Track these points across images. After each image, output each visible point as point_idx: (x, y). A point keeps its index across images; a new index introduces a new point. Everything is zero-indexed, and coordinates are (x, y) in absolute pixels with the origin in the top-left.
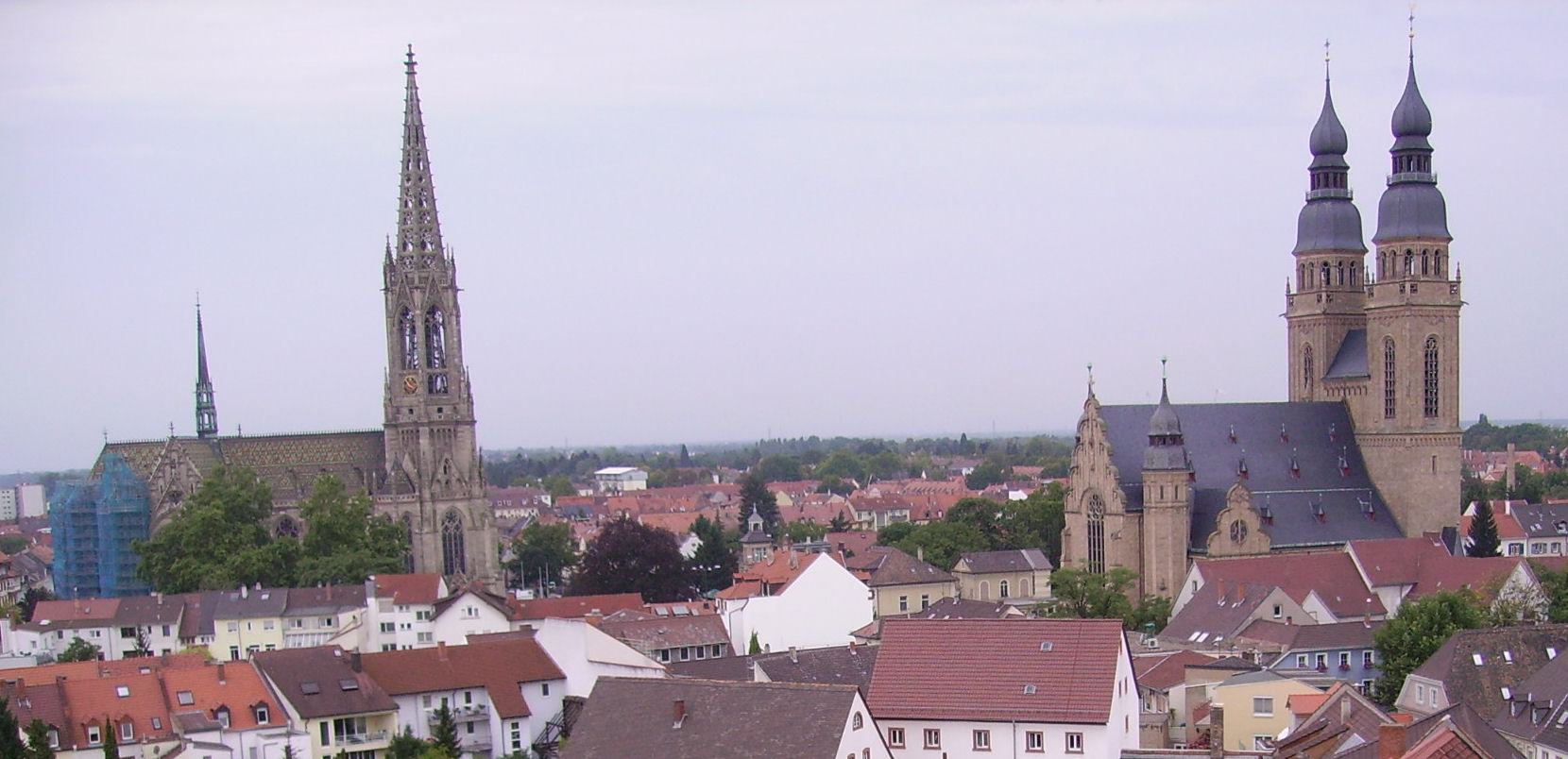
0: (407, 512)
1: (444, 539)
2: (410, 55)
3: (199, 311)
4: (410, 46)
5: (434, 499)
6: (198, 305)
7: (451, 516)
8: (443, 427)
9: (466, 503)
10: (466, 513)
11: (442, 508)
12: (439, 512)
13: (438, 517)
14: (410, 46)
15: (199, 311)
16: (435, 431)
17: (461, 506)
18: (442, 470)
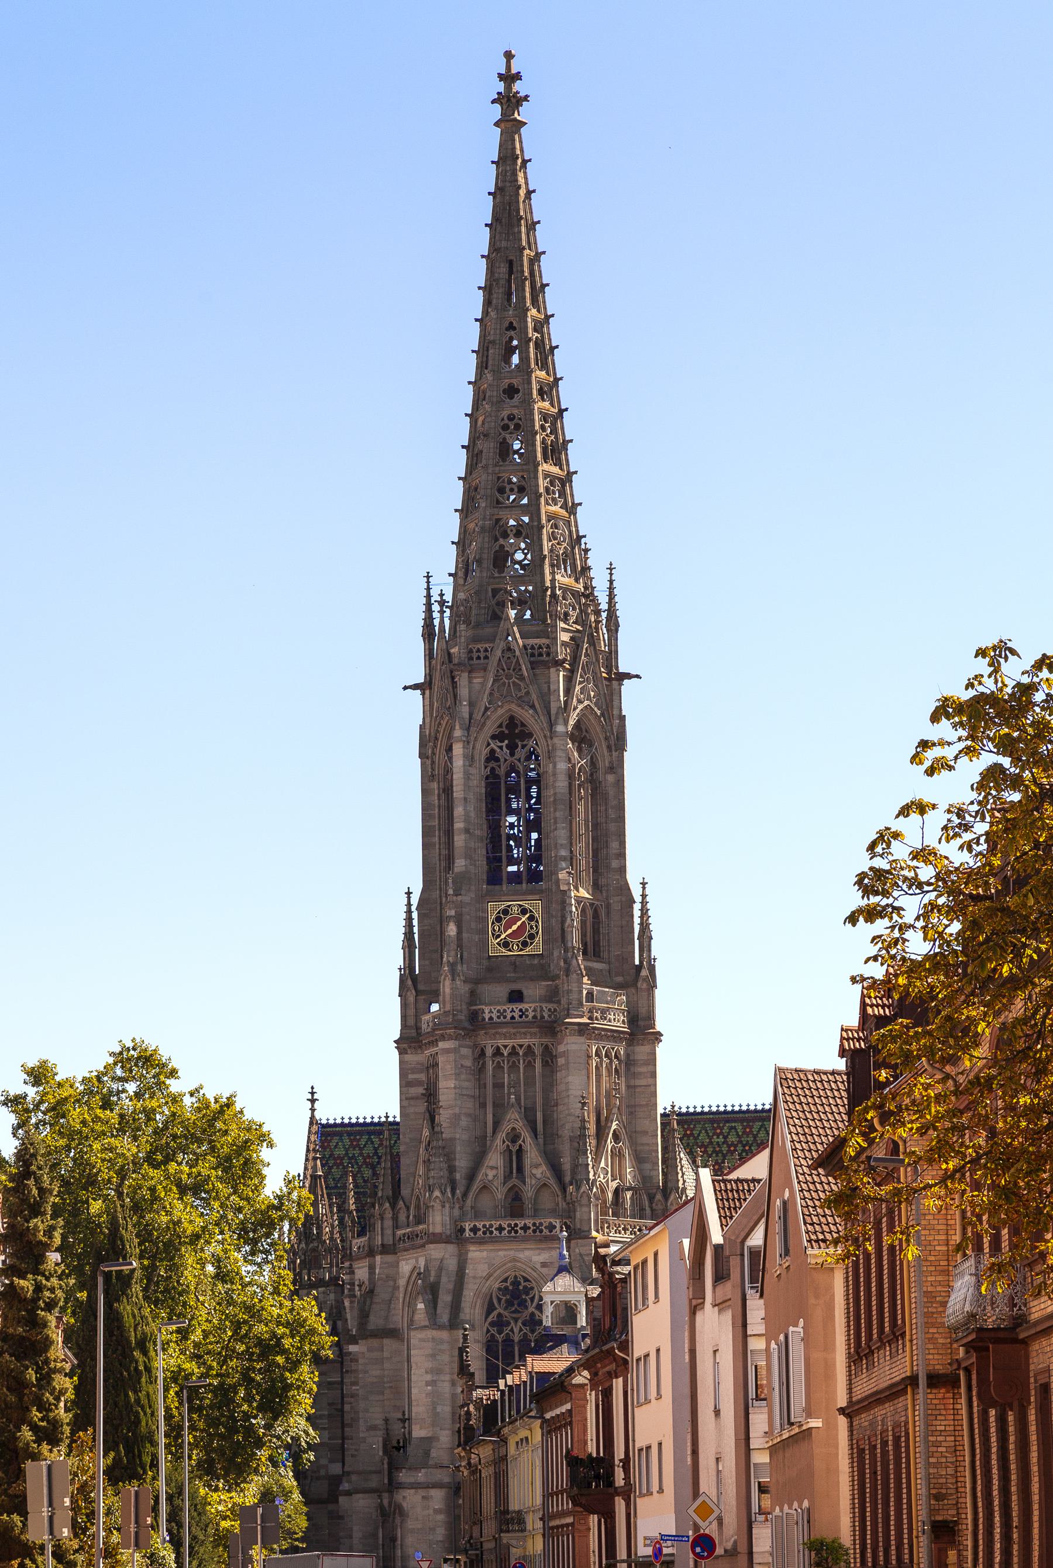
2: (509, 78)
4: (509, 56)
14: (509, 56)
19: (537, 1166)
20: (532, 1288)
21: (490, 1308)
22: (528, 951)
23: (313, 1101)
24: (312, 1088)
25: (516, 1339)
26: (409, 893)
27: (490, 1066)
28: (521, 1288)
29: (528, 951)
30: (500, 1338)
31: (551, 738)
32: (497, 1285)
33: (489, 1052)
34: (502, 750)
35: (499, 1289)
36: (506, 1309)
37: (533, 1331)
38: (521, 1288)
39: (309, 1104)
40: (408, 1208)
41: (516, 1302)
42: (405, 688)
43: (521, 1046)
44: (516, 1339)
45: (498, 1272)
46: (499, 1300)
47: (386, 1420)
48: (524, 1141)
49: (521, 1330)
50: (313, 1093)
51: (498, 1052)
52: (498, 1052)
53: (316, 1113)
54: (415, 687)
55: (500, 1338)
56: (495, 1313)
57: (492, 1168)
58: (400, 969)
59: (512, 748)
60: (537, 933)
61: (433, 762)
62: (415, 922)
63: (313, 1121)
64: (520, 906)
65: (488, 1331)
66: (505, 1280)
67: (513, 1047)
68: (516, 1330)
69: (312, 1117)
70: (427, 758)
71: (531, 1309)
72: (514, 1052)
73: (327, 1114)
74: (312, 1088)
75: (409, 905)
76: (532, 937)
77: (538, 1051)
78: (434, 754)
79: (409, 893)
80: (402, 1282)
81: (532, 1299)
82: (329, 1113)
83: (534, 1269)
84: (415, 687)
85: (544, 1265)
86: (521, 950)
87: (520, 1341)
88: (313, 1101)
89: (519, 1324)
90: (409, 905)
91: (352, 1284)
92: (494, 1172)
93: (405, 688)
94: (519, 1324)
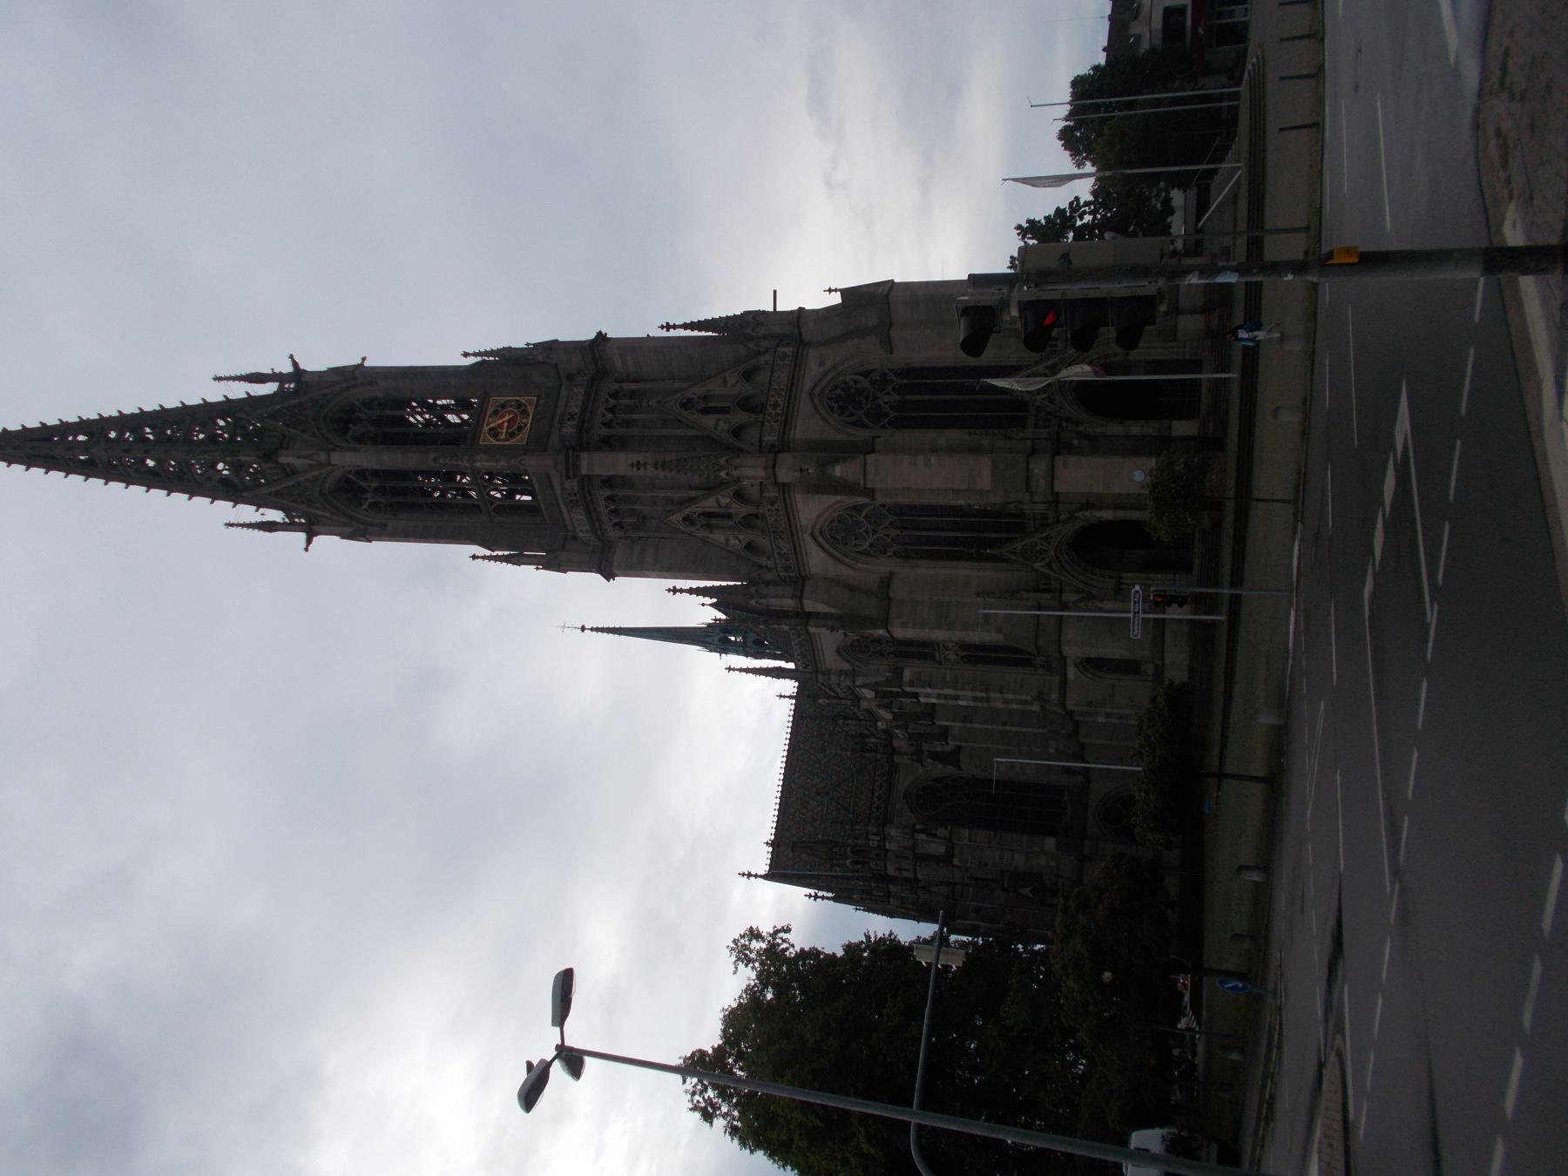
0: (838, 652)
1: (906, 556)
3: (592, 629)
5: (799, 582)
6: (583, 629)
7: (837, 535)
8: (605, 517)
9: (798, 498)
10: (828, 500)
11: (817, 560)
12: (833, 569)
13: (846, 572)
15: (592, 629)
16: (619, 533)
17: (810, 510)
18: (719, 537)
19: (725, 382)
20: (846, 383)
21: (859, 424)
22: (531, 410)
23: (749, 875)
24: (739, 874)
25: (896, 397)
26: (474, 557)
27: (619, 431)
28: (843, 393)
29: (531, 410)
30: (893, 414)
31: (355, 379)
32: (836, 416)
33: (605, 431)
34: (355, 429)
35: (840, 415)
36: (862, 408)
37: (892, 382)
38: (843, 393)
39: (752, 878)
40: (761, 567)
41: (857, 399)
42: (306, 550)
43: (607, 401)
44: (896, 397)
45: (821, 411)
46: (852, 415)
47: (978, 595)
48: (696, 394)
49: (888, 394)
50: (743, 875)
51: (608, 425)
52: (608, 425)
53: (759, 874)
54: (309, 541)
55: (893, 414)
56: (864, 419)
57: (716, 425)
58: (537, 569)
59: (358, 421)
60: (518, 401)
61: (371, 525)
62: (500, 553)
63: (766, 877)
64: (490, 416)
65: (884, 427)
66: (832, 408)
67: (607, 410)
68: (887, 398)
69: (761, 877)
70: (366, 530)
71: (864, 383)
72: (612, 410)
73: (763, 868)
74: (739, 874)
75: (484, 558)
76: (520, 405)
77: (616, 386)
78: (363, 523)
79: (474, 557)
80: (833, 569)
81: (856, 382)
82: (761, 860)
83: (823, 377)
84: (309, 541)
85: (822, 364)
86: (529, 416)
87: (899, 394)
88: (749, 875)
89: (879, 394)
90: (484, 558)
91: (841, 672)
92: (721, 422)
93: (306, 550)
94: (879, 394)
